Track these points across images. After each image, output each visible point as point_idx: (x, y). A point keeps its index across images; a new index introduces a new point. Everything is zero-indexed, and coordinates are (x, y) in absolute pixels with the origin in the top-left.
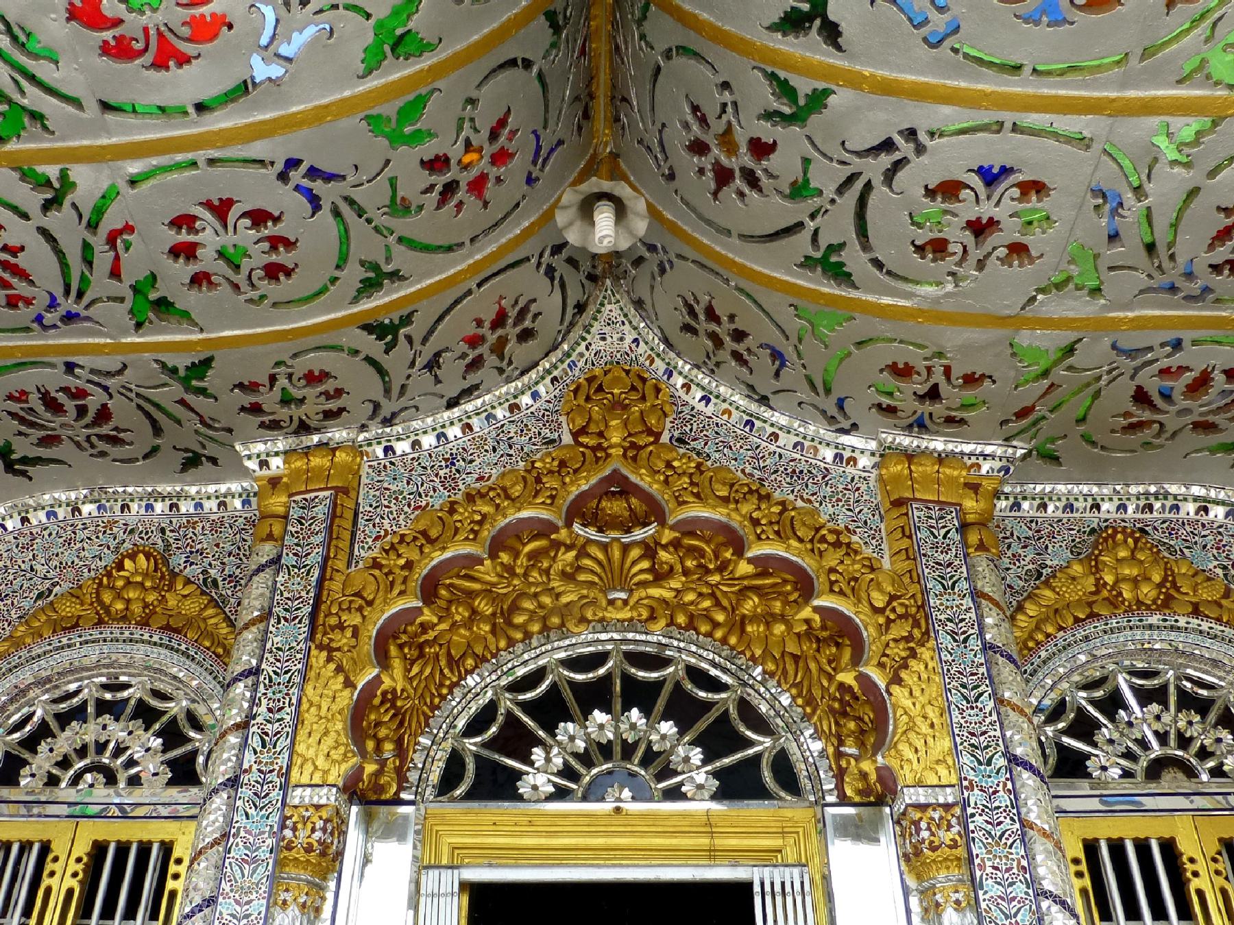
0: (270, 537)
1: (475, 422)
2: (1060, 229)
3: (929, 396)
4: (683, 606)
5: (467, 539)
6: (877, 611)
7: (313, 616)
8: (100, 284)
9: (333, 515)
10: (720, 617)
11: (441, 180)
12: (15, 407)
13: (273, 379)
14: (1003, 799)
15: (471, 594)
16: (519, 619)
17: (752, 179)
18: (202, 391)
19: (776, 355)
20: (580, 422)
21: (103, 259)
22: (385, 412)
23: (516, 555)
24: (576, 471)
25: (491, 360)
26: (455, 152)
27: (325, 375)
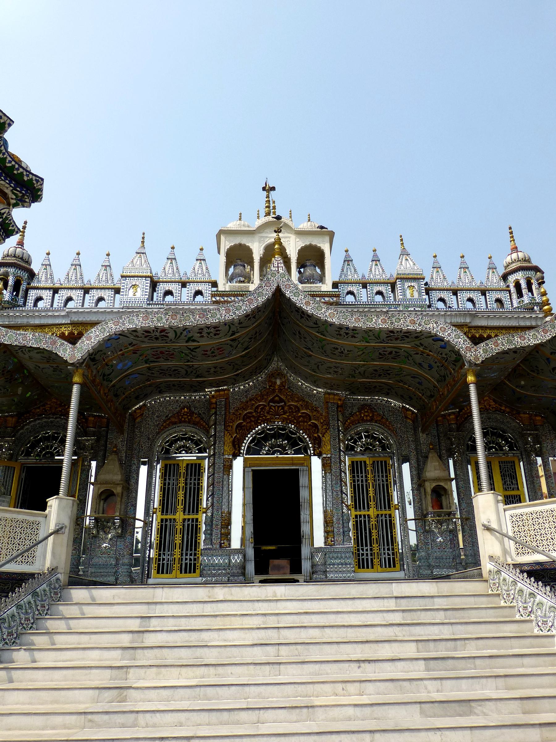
6: (322, 423)
7: (224, 424)
9: (226, 404)
14: (338, 456)
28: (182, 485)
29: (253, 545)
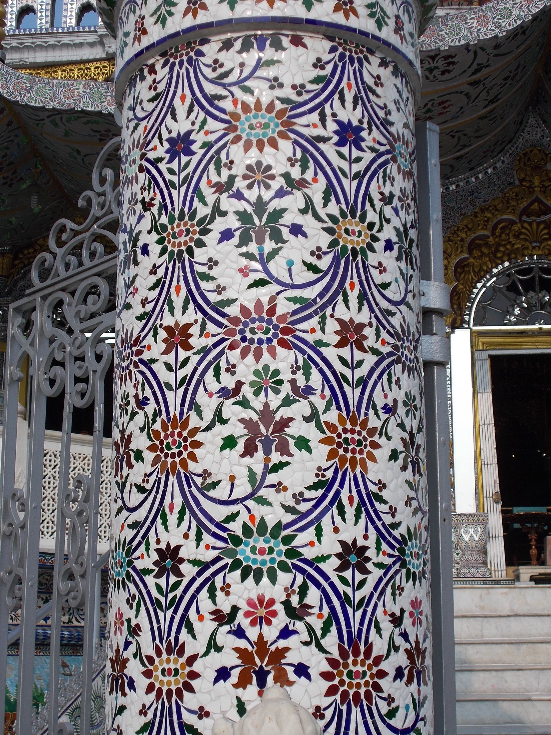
5: (483, 228)
16: (499, 255)
20: (522, 176)
24: (522, 198)
29: (499, 506)
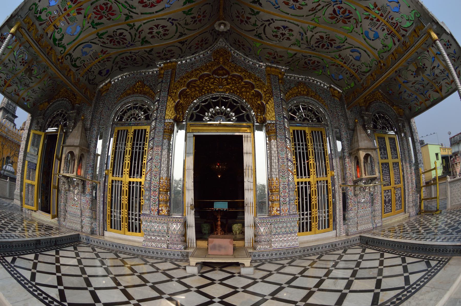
0: (161, 77)
1: (197, 57)
2: (296, 36)
3: (274, 58)
4: (232, 89)
6: (264, 92)
8: (137, 39)
9: (172, 73)
10: (238, 91)
11: (194, 20)
12: (122, 60)
13: (163, 51)
15: (195, 86)
16: (204, 91)
17: (246, 22)
18: (151, 54)
19: (250, 49)
20: (215, 58)
21: (138, 36)
22: (181, 56)
23: (203, 80)
25: (200, 47)
26: (197, 16)
27: (172, 50)
28: (129, 148)
